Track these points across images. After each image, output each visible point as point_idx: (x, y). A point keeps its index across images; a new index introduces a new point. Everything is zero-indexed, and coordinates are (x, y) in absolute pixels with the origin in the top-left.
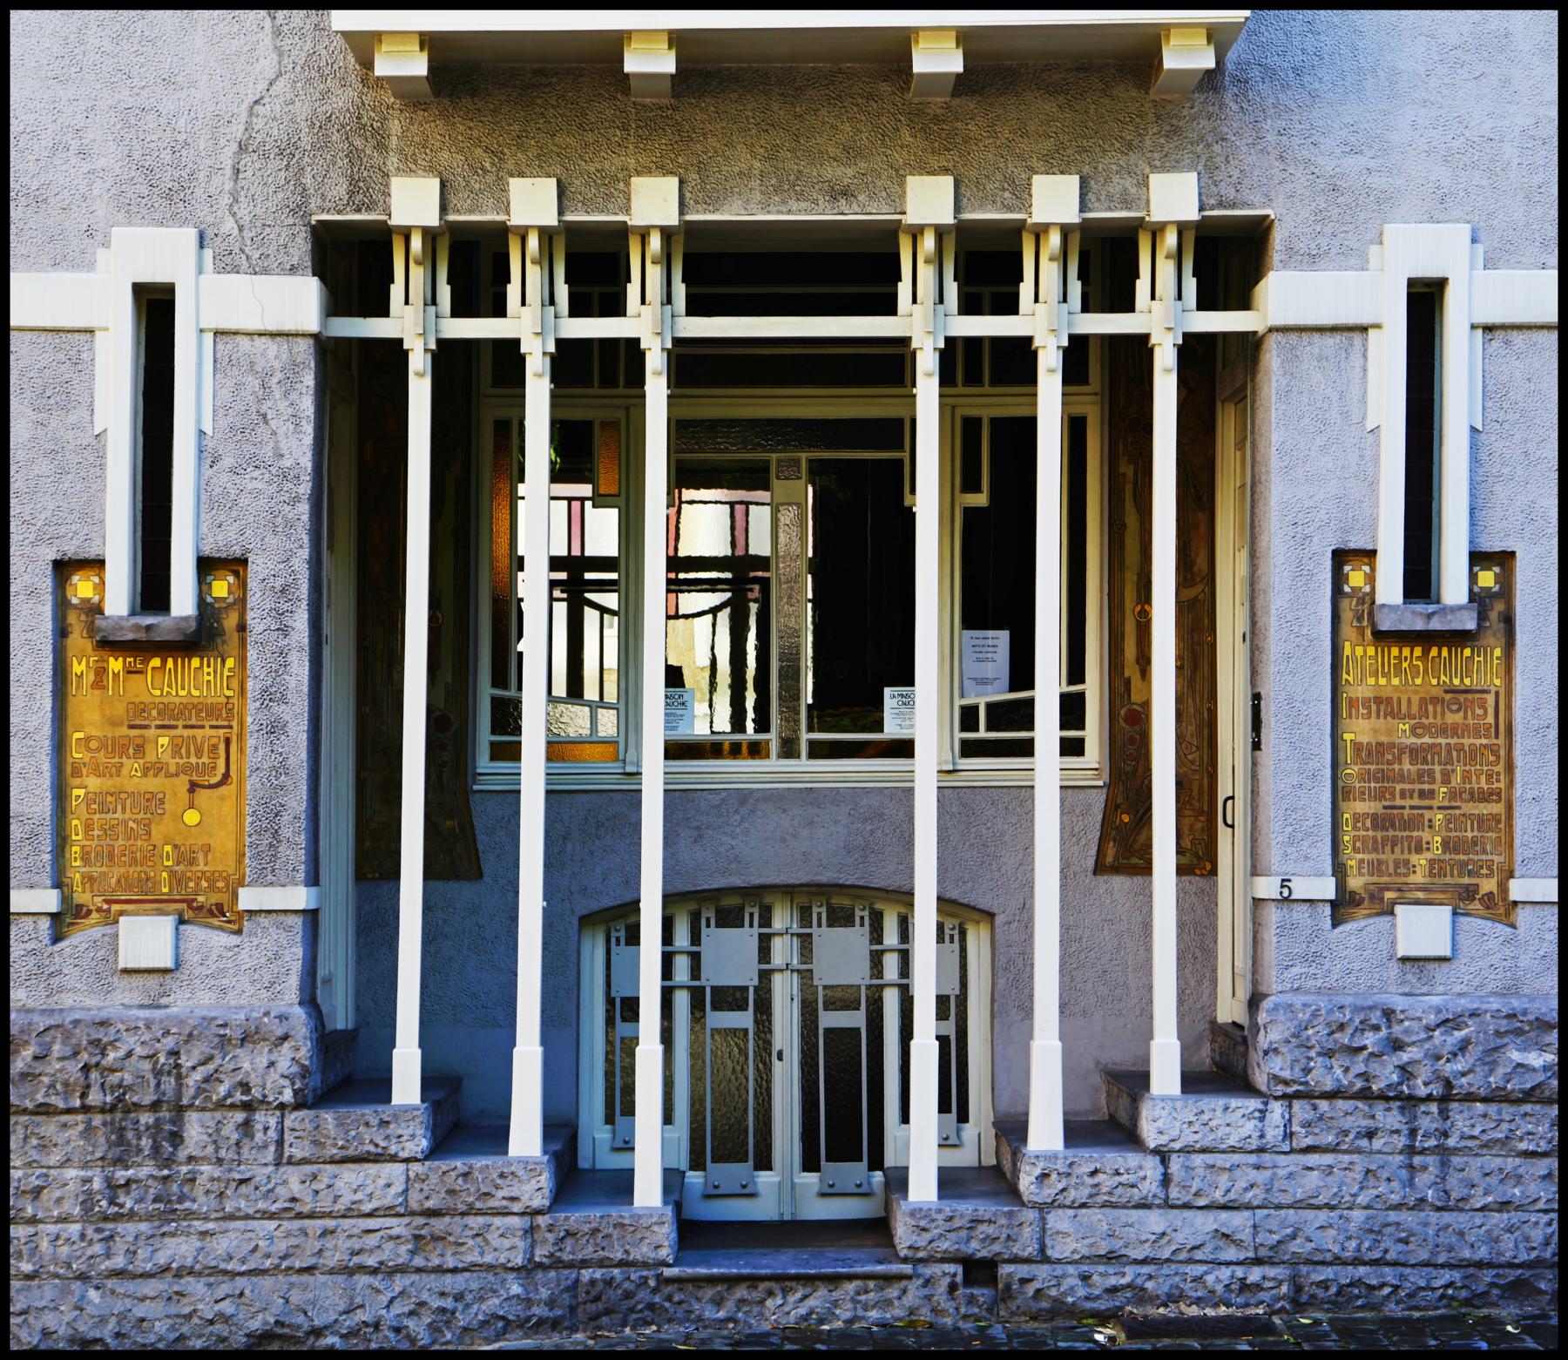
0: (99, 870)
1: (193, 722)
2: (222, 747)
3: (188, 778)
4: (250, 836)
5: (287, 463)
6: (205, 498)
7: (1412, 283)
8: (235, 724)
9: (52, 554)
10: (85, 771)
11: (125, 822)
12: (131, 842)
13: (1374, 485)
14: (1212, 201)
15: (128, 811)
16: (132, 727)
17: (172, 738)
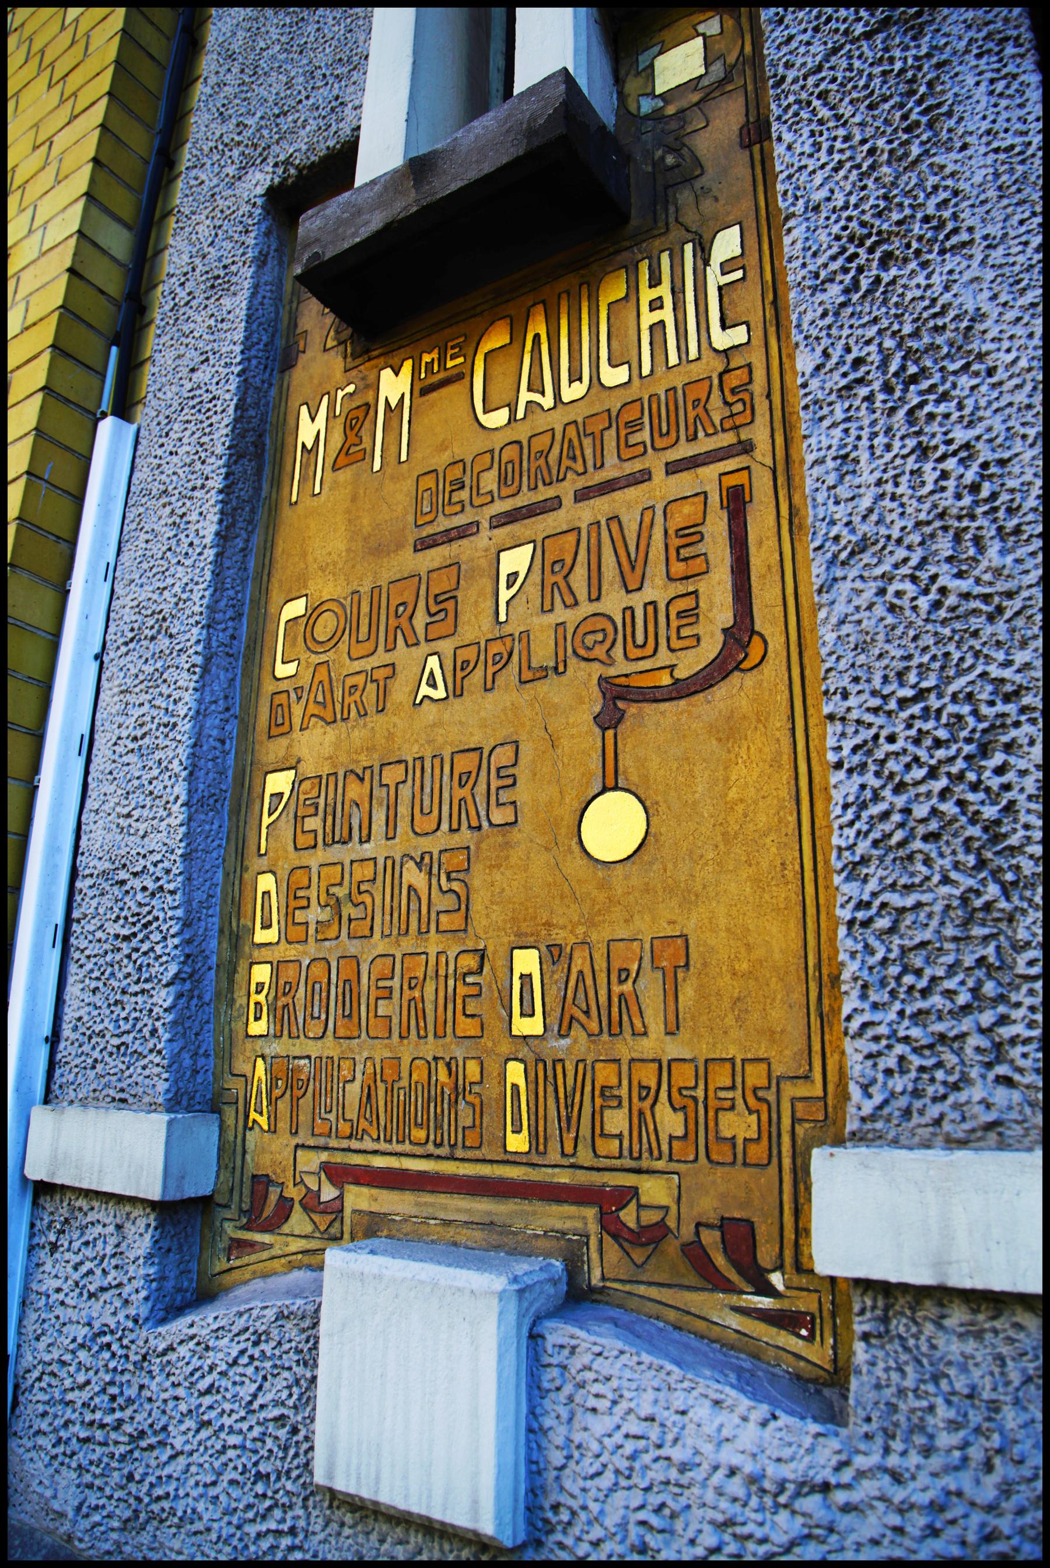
0: (314, 1049)
1: (610, 472)
2: (717, 526)
3: (596, 670)
4: (854, 870)
8: (759, 433)
10: (297, 711)
11: (394, 866)
12: (408, 944)
15: (403, 826)
16: (424, 545)
17: (540, 547)
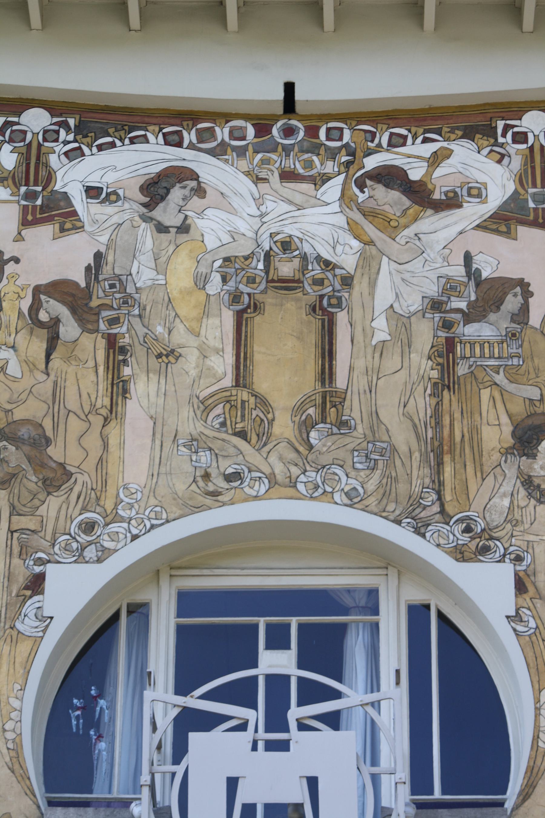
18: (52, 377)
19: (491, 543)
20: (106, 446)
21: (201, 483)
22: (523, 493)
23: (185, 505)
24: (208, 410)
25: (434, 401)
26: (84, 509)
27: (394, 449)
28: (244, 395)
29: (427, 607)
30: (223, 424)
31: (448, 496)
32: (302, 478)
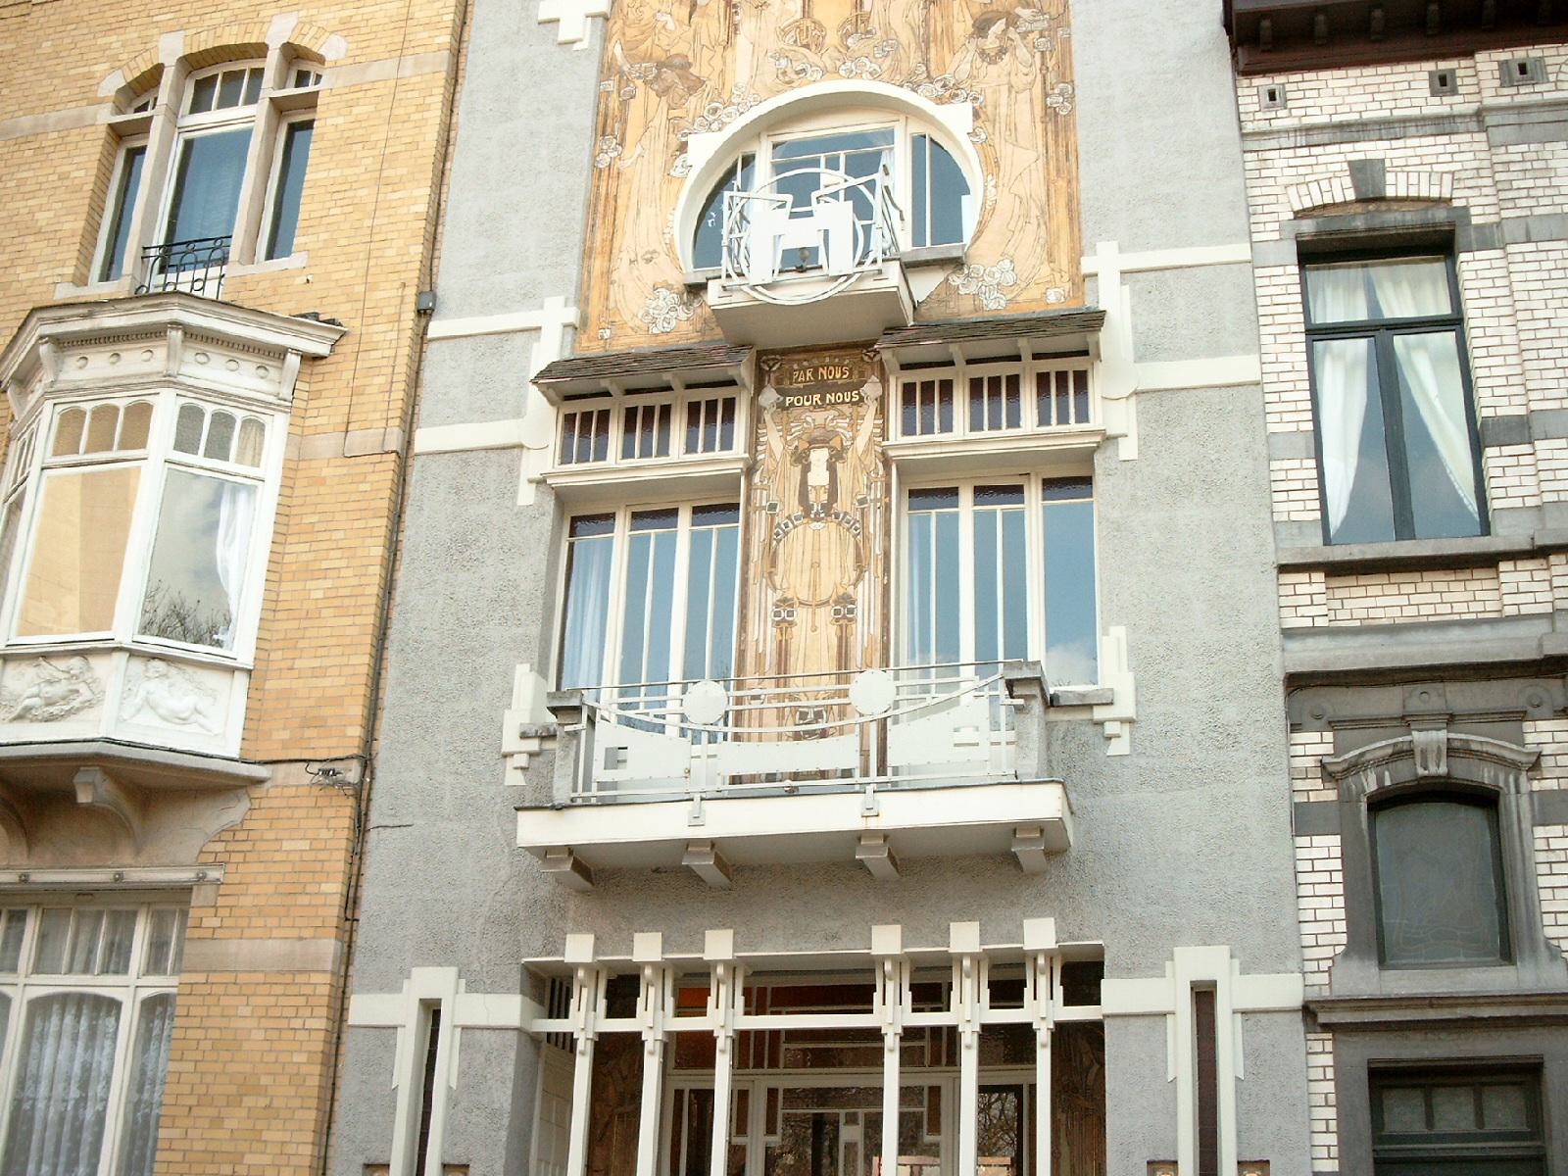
5: (496, 1106)
6: (450, 1129)
7: (1194, 986)
9: (361, 1160)
13: (1174, 1115)
14: (1065, 936)
18: (693, 27)
19: (959, 92)
20: (724, 63)
21: (781, 78)
22: (979, 60)
23: (771, 91)
24: (786, 34)
25: (925, 11)
26: (712, 101)
27: (899, 43)
28: (808, 23)
29: (925, 137)
30: (795, 41)
31: (932, 67)
32: (843, 67)
